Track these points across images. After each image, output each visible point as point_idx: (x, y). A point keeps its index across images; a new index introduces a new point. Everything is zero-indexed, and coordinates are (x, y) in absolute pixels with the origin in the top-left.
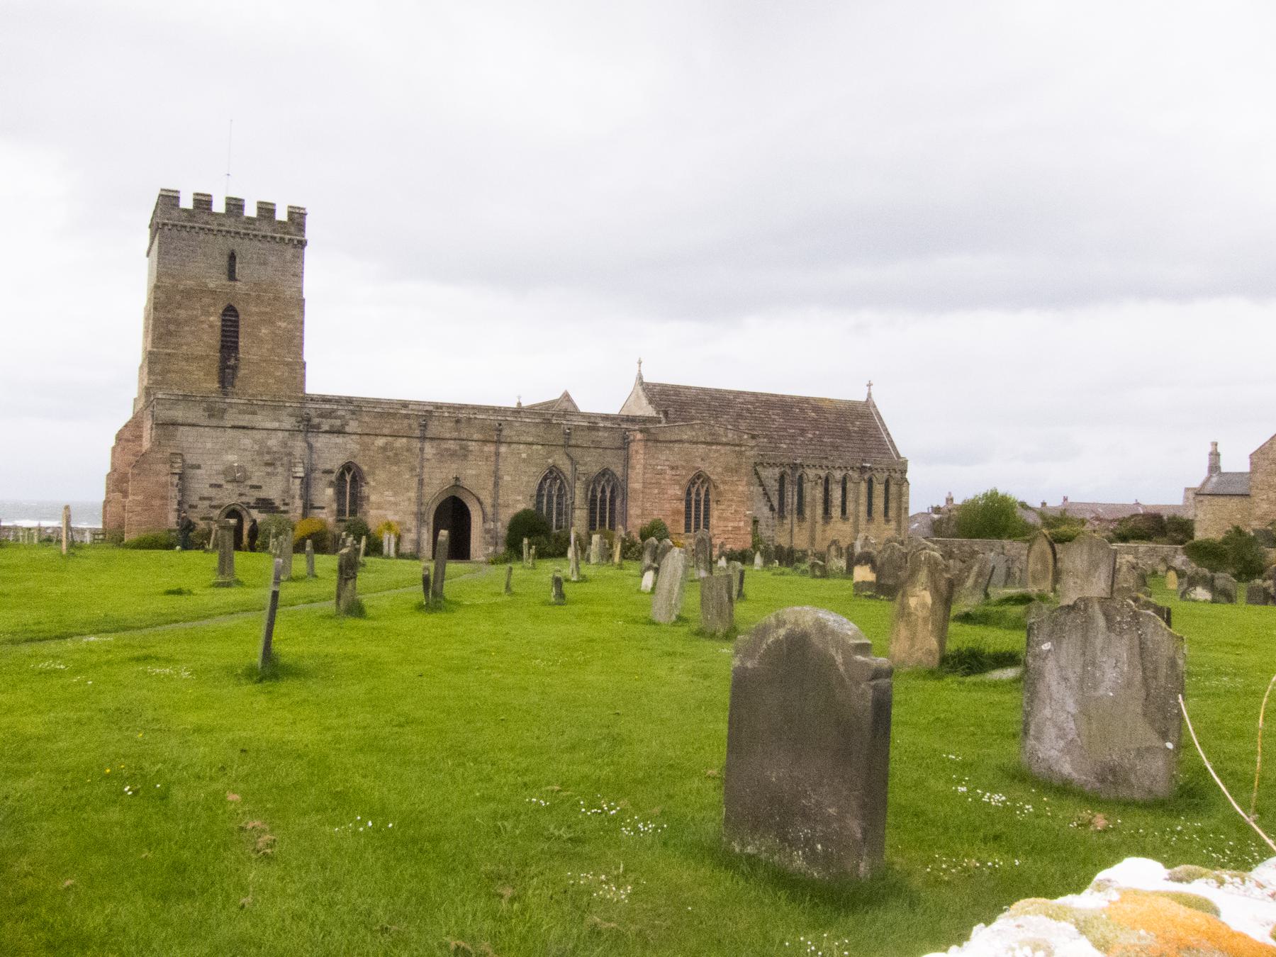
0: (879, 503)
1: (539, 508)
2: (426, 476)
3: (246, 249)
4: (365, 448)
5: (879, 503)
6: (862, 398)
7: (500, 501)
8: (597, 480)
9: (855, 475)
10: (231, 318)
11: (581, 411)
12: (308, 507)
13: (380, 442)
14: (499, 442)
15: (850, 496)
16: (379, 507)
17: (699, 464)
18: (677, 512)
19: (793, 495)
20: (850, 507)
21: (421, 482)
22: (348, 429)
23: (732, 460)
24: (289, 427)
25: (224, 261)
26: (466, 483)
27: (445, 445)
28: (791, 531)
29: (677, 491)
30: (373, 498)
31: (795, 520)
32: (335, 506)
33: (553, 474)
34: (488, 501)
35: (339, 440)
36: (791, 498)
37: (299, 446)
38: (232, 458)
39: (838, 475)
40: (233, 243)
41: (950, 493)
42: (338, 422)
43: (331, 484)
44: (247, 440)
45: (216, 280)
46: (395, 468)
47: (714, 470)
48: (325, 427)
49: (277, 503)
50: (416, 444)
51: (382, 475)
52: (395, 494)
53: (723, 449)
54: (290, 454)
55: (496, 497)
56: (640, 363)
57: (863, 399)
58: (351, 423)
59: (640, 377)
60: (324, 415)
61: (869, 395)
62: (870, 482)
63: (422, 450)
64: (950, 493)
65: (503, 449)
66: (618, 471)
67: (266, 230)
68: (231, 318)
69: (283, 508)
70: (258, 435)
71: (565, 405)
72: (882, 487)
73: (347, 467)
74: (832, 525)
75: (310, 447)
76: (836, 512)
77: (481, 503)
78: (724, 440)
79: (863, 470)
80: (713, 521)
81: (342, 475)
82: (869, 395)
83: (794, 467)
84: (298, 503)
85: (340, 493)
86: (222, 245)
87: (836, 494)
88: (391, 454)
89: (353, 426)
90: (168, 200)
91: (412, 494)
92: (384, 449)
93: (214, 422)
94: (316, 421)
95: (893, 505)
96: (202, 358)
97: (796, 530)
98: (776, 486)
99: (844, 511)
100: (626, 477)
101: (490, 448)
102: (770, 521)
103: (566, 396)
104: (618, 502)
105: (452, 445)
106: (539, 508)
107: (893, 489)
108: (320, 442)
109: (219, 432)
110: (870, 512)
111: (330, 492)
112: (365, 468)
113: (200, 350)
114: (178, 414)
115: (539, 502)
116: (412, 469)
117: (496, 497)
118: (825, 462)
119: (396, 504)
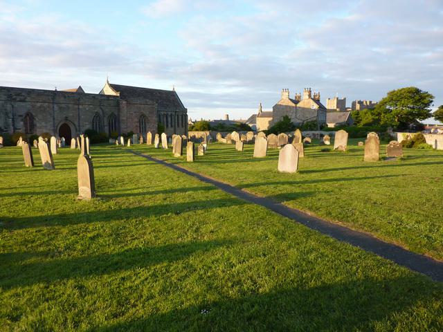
0: (180, 122)
1: (93, 127)
2: (55, 117)
4: (33, 106)
5: (180, 122)
6: (172, 90)
7: (81, 125)
8: (110, 116)
9: (174, 113)
11: (86, 92)
12: (15, 129)
13: (39, 105)
14: (78, 105)
15: (173, 120)
16: (40, 128)
18: (137, 126)
20: (173, 124)
21: (54, 119)
22: (27, 100)
24: (3, 99)
26: (69, 118)
29: (136, 120)
30: (38, 125)
32: (24, 128)
33: (97, 115)
34: (76, 123)
35: (24, 104)
37: (9, 107)
39: (169, 113)
42: (22, 98)
43: (22, 120)
46: (44, 114)
47: (146, 113)
48: (18, 99)
49: (3, 128)
50: (51, 105)
51: (40, 116)
52: (46, 123)
54: (6, 110)
55: (79, 124)
58: (28, 98)
60: (19, 95)
63: (53, 107)
65: (81, 107)
66: (116, 114)
69: (5, 130)
71: (80, 91)
73: (27, 114)
75: (13, 106)
76: (169, 125)
77: (75, 125)
79: (176, 112)
81: (26, 117)
84: (12, 127)
85: (25, 124)
87: (169, 119)
88: (42, 109)
89: (28, 99)
91: (52, 123)
92: (40, 107)
94: (14, 97)
95: (184, 122)
100: (119, 115)
101: (76, 107)
103: (80, 87)
104: (117, 124)
105: (63, 105)
106: (95, 129)
107: (184, 117)
108: (17, 105)
111: (22, 123)
112: (34, 114)
115: (93, 125)
116: (51, 114)
117: (79, 124)
119: (46, 126)
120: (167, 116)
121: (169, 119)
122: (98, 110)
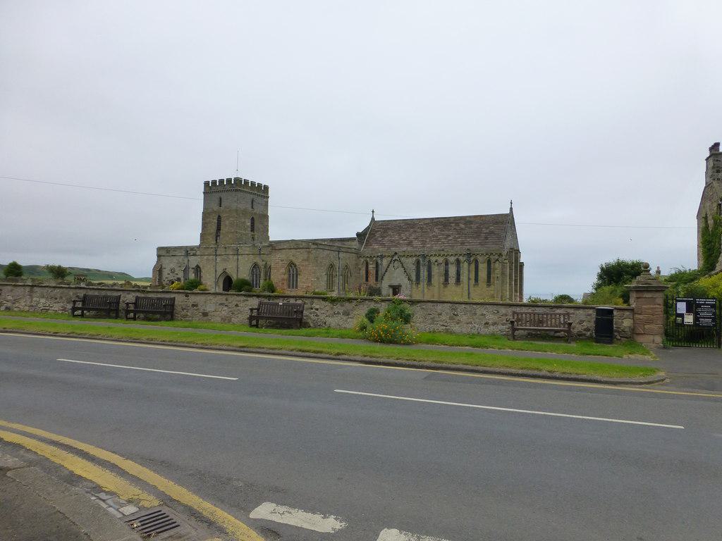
0: (483, 274)
3: (223, 195)
5: (483, 274)
10: (219, 219)
13: (205, 257)
17: (292, 258)
19: (424, 272)
20: (464, 278)
23: (306, 256)
25: (218, 202)
27: (223, 257)
28: (424, 291)
29: (283, 270)
31: (426, 286)
33: (255, 266)
35: (195, 257)
36: (424, 273)
38: (172, 266)
39: (452, 259)
40: (220, 194)
41: (658, 267)
44: (175, 259)
45: (216, 207)
53: (302, 251)
56: (373, 212)
57: (508, 212)
59: (373, 219)
61: (511, 209)
62: (476, 262)
64: (658, 267)
65: (240, 257)
67: (228, 188)
68: (219, 219)
70: (178, 258)
72: (485, 265)
73: (198, 267)
74: (449, 287)
76: (452, 280)
78: (301, 246)
80: (300, 284)
82: (511, 209)
83: (424, 257)
86: (218, 195)
87: (452, 270)
89: (198, 253)
90: (206, 184)
93: (168, 254)
96: (211, 234)
97: (426, 291)
98: (414, 267)
99: (458, 280)
101: (236, 257)
102: (409, 286)
108: (192, 258)
109: (169, 258)
110: (476, 280)
113: (212, 231)
114: (163, 253)
118: (442, 253)
120: (447, 264)
121: (452, 270)
122: (258, 260)
